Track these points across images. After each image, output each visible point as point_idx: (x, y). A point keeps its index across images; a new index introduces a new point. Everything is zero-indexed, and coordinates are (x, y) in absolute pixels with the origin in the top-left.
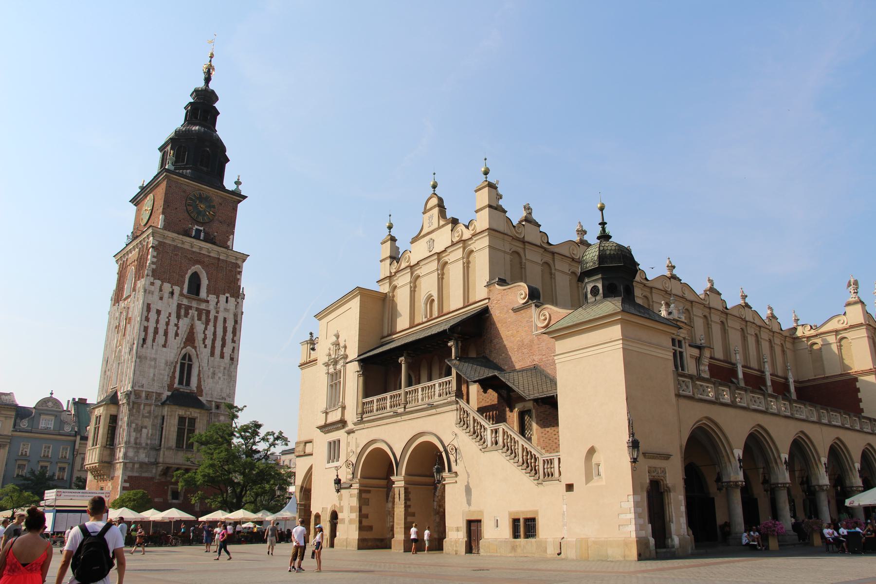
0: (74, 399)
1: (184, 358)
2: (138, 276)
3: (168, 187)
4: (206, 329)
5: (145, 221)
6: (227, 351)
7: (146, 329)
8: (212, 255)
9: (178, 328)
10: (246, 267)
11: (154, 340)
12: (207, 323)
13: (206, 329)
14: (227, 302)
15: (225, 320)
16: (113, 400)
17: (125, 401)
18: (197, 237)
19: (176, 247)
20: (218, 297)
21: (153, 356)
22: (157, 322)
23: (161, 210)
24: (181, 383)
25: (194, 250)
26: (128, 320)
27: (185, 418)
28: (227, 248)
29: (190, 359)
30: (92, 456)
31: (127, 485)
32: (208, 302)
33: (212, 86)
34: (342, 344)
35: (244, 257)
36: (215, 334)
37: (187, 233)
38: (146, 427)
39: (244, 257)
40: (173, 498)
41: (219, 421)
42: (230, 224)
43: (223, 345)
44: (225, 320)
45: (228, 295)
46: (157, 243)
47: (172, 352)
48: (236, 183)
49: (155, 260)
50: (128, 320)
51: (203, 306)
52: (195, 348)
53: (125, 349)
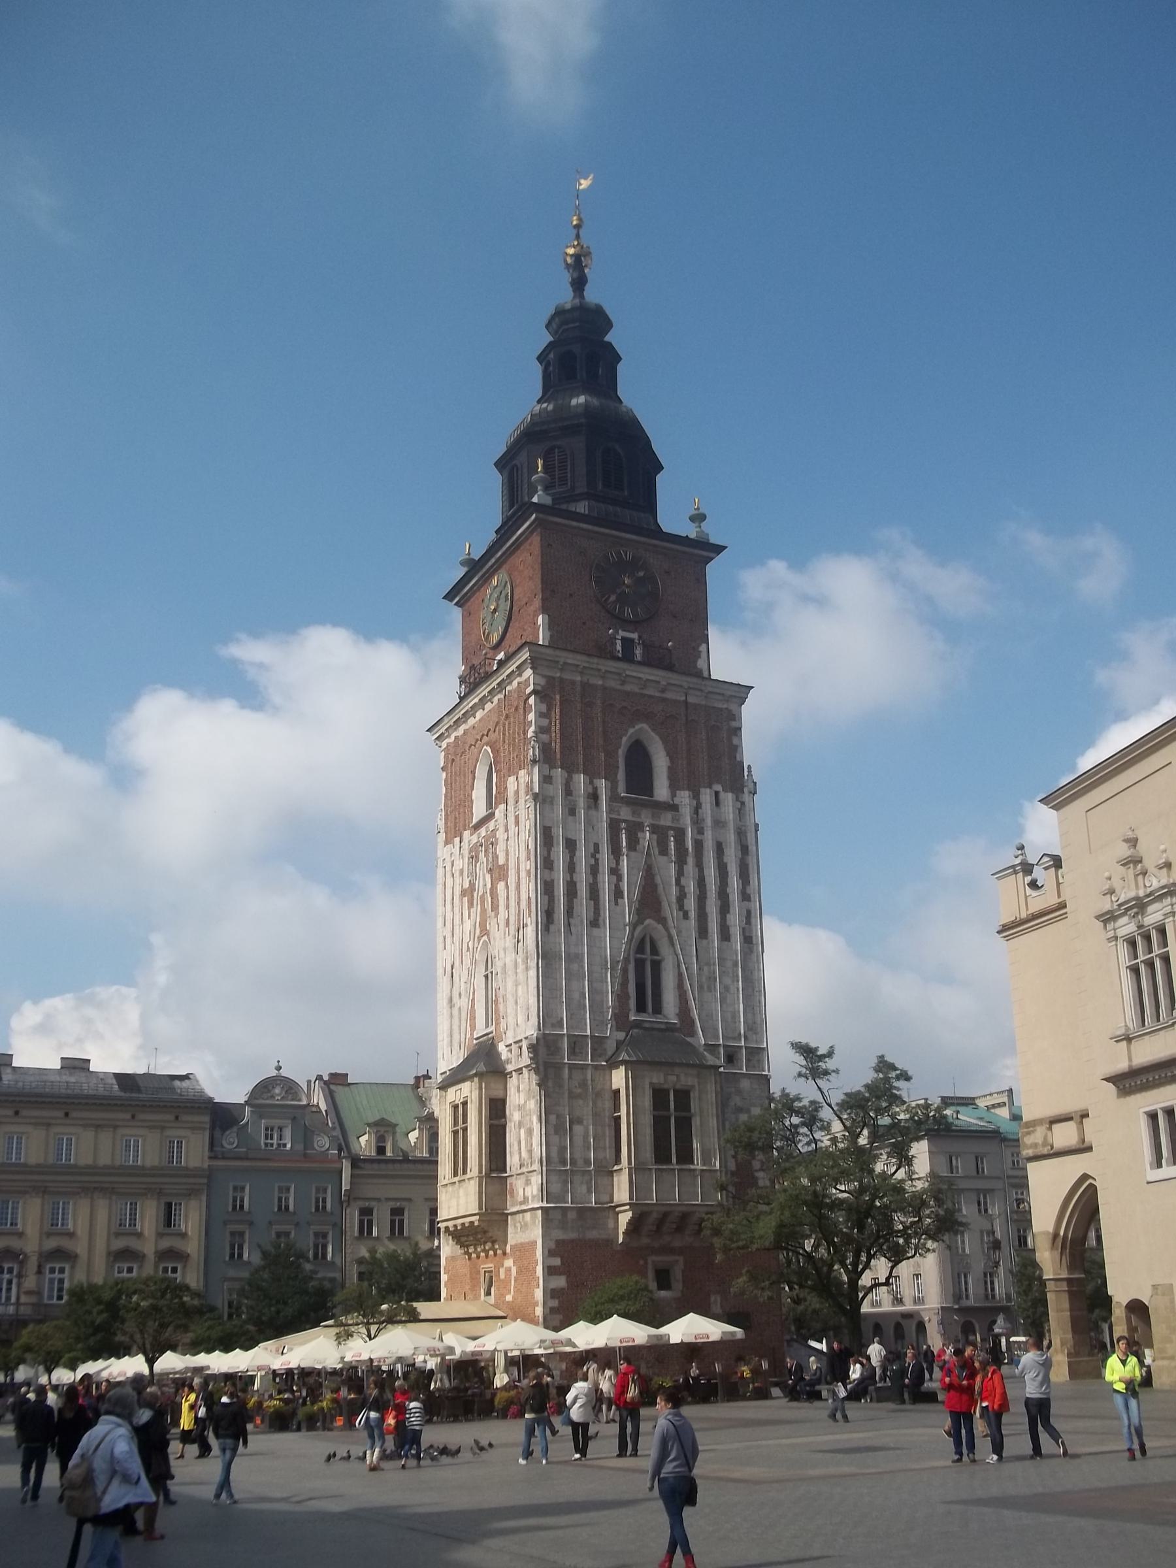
0: (319, 1078)
1: (640, 948)
2: (499, 770)
3: (546, 547)
4: (680, 873)
5: (495, 638)
6: (735, 920)
7: (548, 888)
8: (669, 695)
9: (620, 878)
10: (750, 713)
12: (681, 861)
13: (680, 873)
14: (717, 803)
15: (720, 848)
16: (484, 1062)
17: (526, 1060)
18: (628, 656)
19: (585, 685)
20: (696, 796)
21: (573, 950)
22: (571, 868)
23: (537, 603)
24: (641, 1008)
25: (628, 688)
26: (498, 872)
27: (667, 1092)
28: (698, 674)
29: (655, 951)
30: (458, 1200)
31: (557, 1262)
32: (674, 808)
33: (592, 295)
34: (1150, 863)
35: (740, 692)
36: (701, 883)
37: (604, 651)
38: (579, 1121)
39: (740, 692)
40: (660, 1288)
41: (739, 1092)
43: (724, 909)
45: (718, 787)
46: (543, 682)
48: (693, 519)
49: (545, 722)
50: (498, 872)
51: (666, 820)
52: (663, 921)
53: (501, 941)
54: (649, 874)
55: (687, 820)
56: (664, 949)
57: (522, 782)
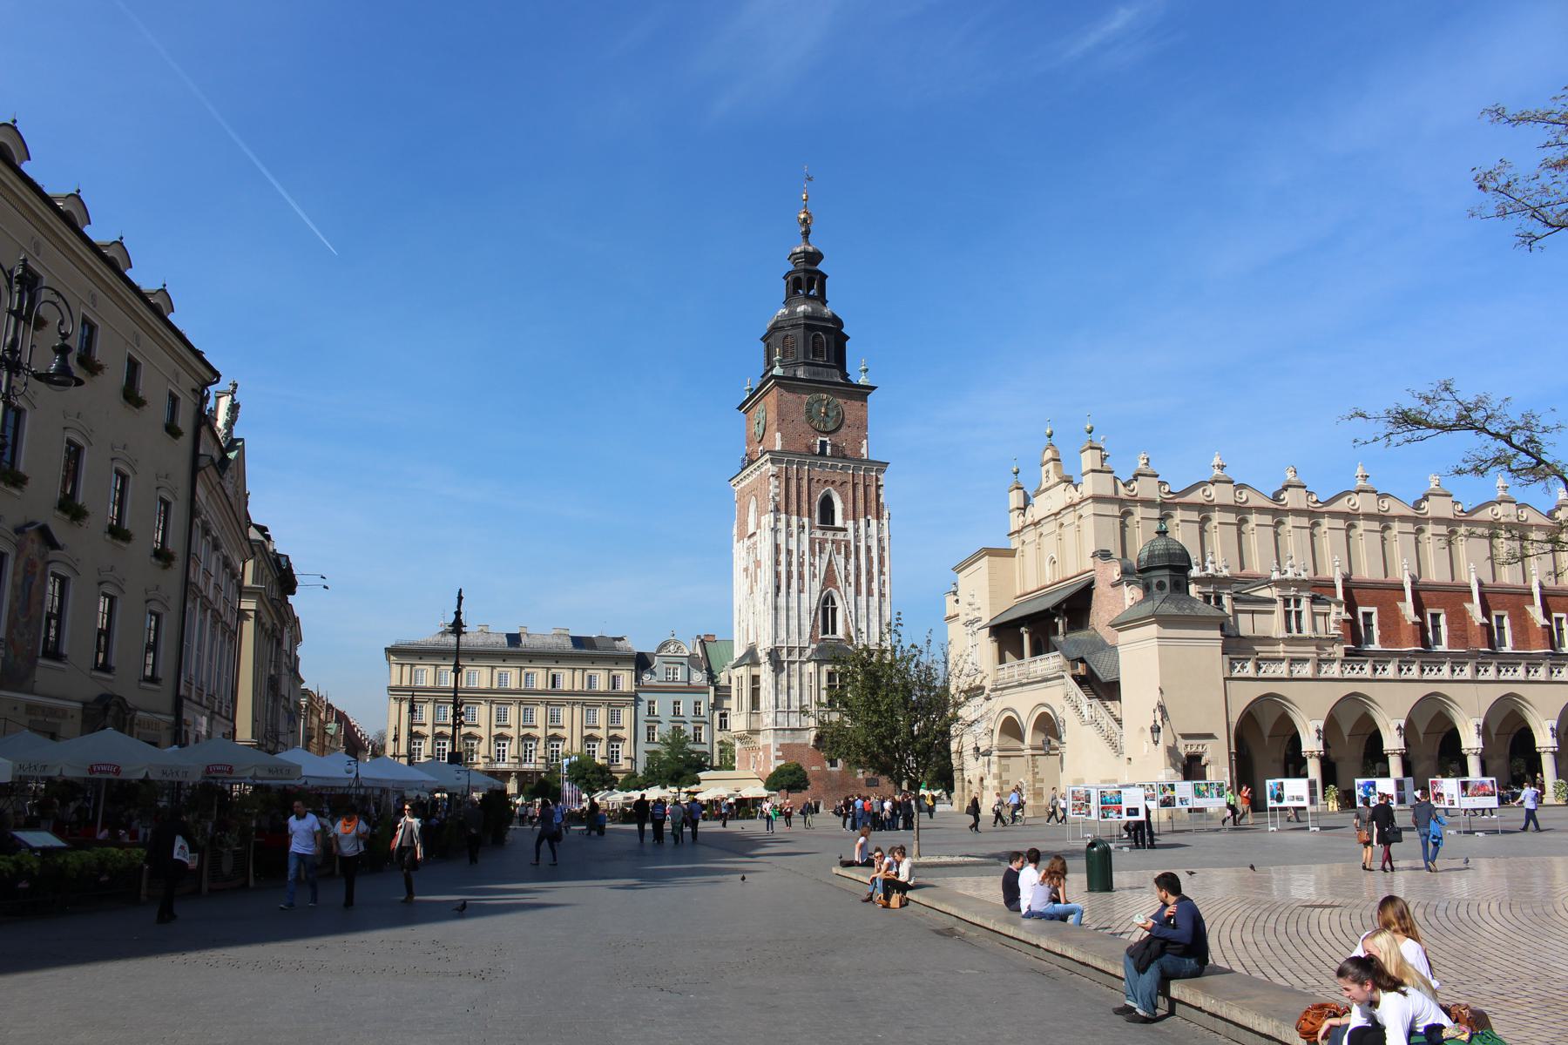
1: (826, 602)
7: (777, 575)
11: (788, 586)
12: (847, 558)
15: (869, 549)
22: (789, 564)
24: (825, 632)
29: (833, 603)
32: (845, 530)
36: (858, 568)
42: (862, 426)
43: (870, 580)
44: (869, 549)
47: (811, 599)
51: (840, 536)
52: (838, 588)
54: (830, 561)
55: (851, 535)
56: (838, 603)
57: (768, 519)
